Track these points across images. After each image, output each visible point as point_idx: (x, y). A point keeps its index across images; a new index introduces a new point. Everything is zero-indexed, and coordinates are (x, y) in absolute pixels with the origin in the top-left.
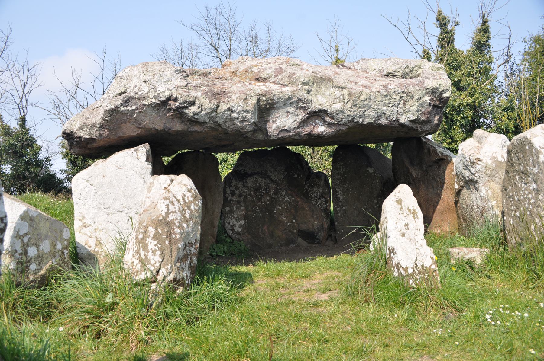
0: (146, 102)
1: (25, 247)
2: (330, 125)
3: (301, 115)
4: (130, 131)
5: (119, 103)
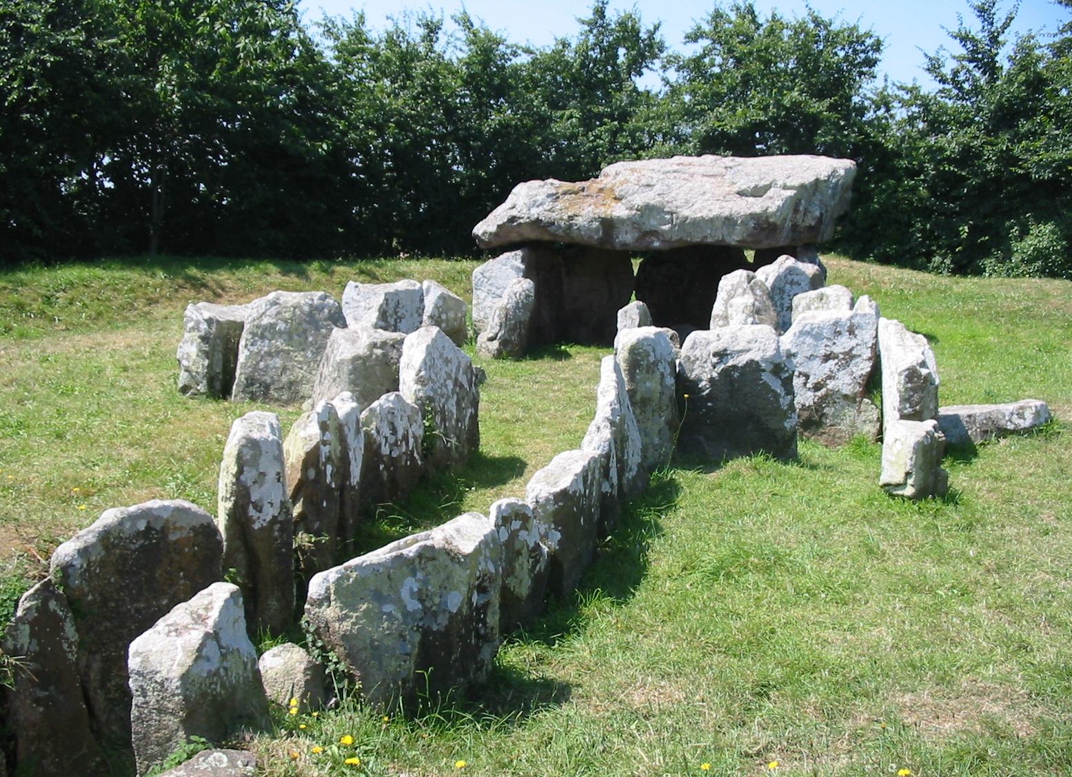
0: (522, 221)
1: (440, 314)
2: (664, 241)
3: (637, 235)
4: (514, 237)
5: (505, 220)
